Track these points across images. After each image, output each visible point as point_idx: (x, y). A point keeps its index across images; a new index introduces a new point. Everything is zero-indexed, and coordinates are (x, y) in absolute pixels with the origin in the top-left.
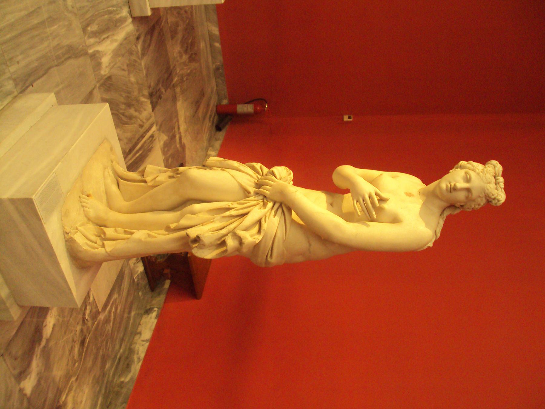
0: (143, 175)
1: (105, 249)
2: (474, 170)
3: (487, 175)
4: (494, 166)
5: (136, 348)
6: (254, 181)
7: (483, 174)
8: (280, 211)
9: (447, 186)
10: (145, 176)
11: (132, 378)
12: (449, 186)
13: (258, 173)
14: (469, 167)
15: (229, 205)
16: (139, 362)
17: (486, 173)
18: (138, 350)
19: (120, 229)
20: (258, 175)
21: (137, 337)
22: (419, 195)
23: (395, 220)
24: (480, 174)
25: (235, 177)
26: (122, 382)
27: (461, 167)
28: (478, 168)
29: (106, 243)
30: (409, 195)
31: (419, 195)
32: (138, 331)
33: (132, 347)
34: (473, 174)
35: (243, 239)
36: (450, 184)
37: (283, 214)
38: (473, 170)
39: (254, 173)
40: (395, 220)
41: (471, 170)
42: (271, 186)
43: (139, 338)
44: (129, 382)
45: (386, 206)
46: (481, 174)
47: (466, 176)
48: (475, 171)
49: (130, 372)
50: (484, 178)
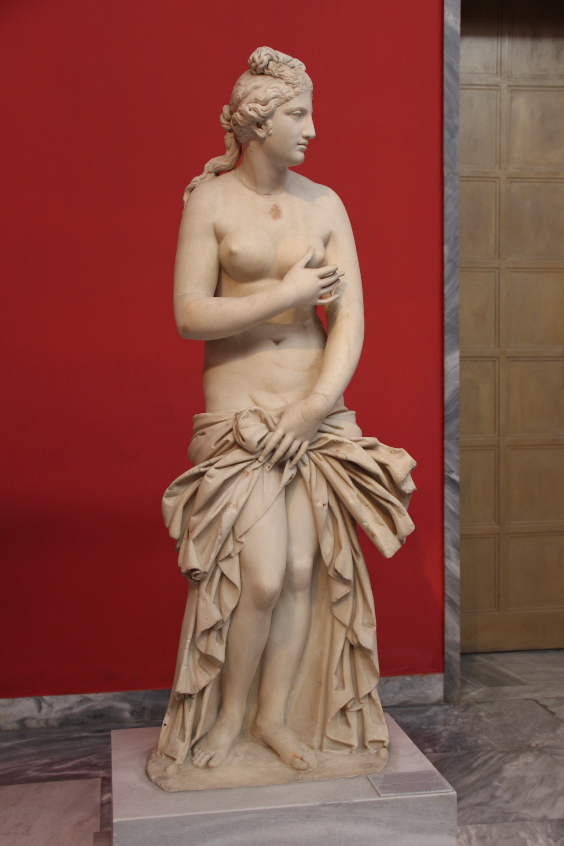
0: (190, 696)
1: (373, 690)
2: (289, 99)
3: (300, 82)
4: (269, 61)
5: (59, 715)
6: (268, 474)
7: (298, 86)
8: (334, 421)
9: (301, 150)
10: (193, 693)
11: (124, 700)
12: (303, 147)
13: (242, 471)
14: (276, 105)
15: (324, 505)
16: (89, 700)
17: (297, 81)
18: (60, 710)
19: (335, 681)
20: (249, 470)
21: (32, 724)
22: (271, 196)
23: (326, 242)
24: (299, 92)
25: (269, 506)
26: (132, 713)
27: (271, 115)
28: (285, 91)
29: (364, 691)
30: (276, 213)
31: (270, 195)
32: (16, 726)
33: (55, 724)
34: (295, 104)
35: (412, 466)
36: (298, 144)
37: (331, 417)
38: (287, 100)
39: (247, 475)
40: (326, 242)
41: (283, 103)
42: (294, 439)
43: (32, 718)
44: (130, 702)
45: (319, 254)
46: (297, 89)
47: (296, 114)
48: (291, 98)
49: (110, 708)
50: (304, 87)
